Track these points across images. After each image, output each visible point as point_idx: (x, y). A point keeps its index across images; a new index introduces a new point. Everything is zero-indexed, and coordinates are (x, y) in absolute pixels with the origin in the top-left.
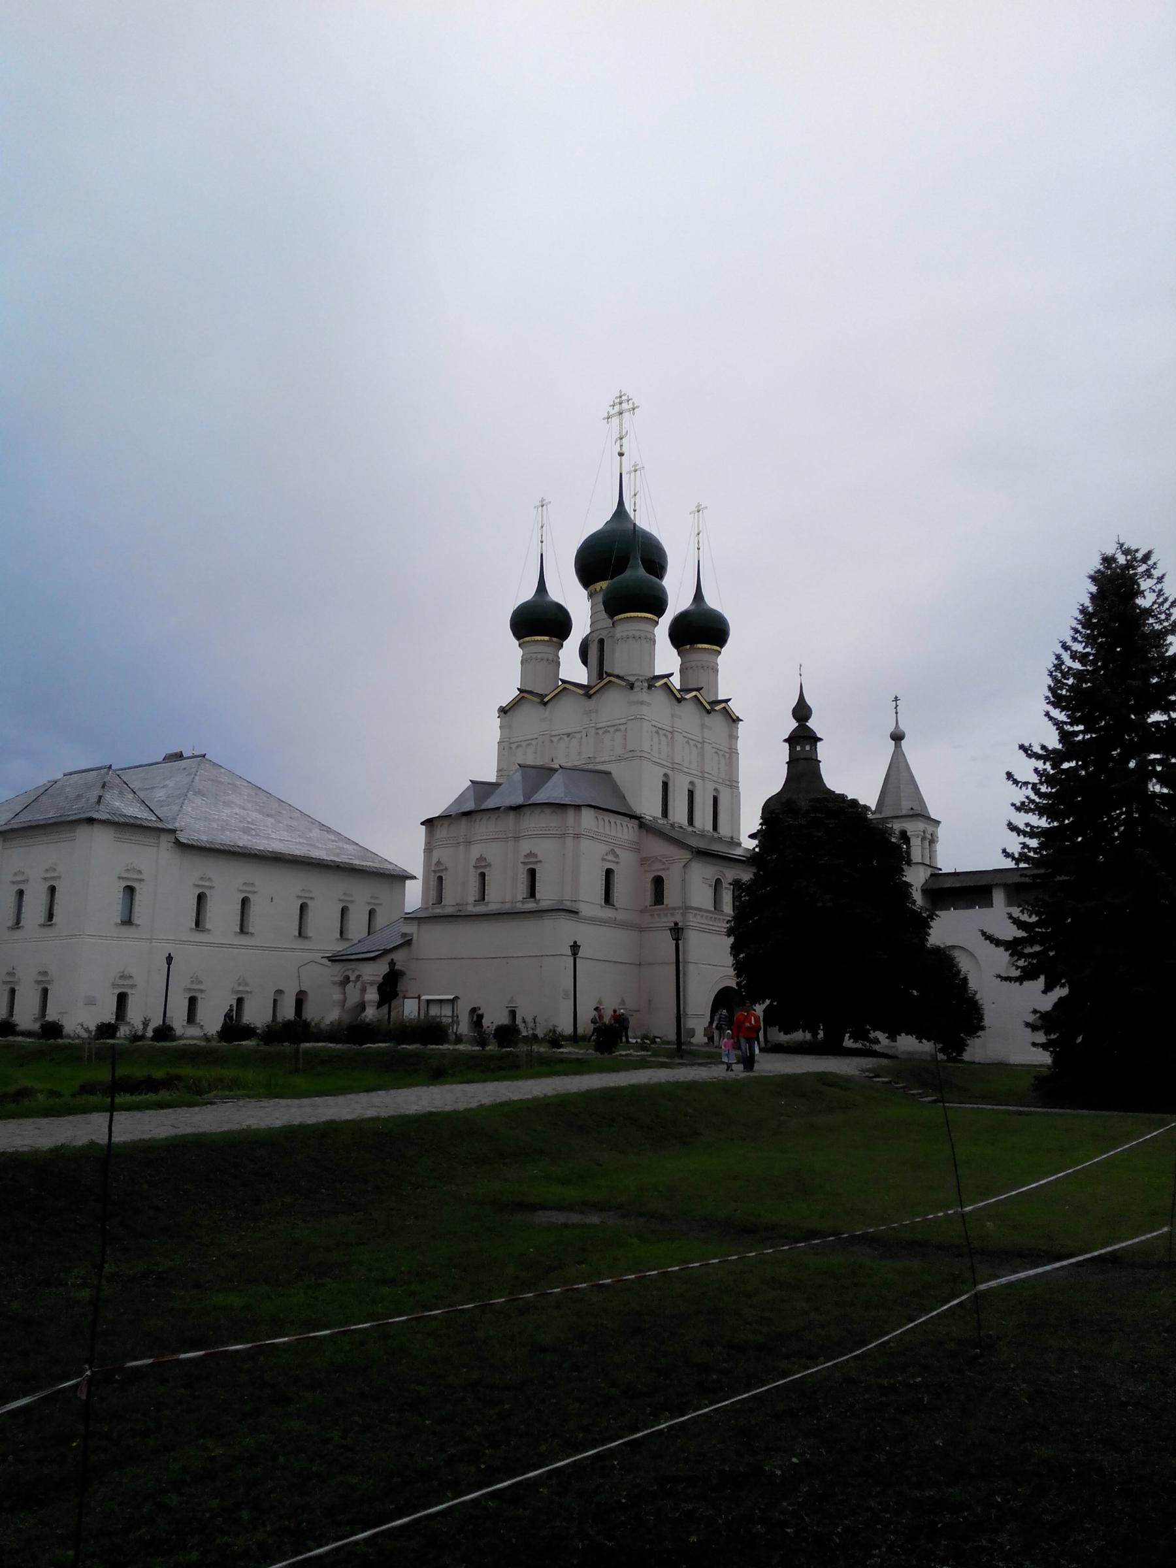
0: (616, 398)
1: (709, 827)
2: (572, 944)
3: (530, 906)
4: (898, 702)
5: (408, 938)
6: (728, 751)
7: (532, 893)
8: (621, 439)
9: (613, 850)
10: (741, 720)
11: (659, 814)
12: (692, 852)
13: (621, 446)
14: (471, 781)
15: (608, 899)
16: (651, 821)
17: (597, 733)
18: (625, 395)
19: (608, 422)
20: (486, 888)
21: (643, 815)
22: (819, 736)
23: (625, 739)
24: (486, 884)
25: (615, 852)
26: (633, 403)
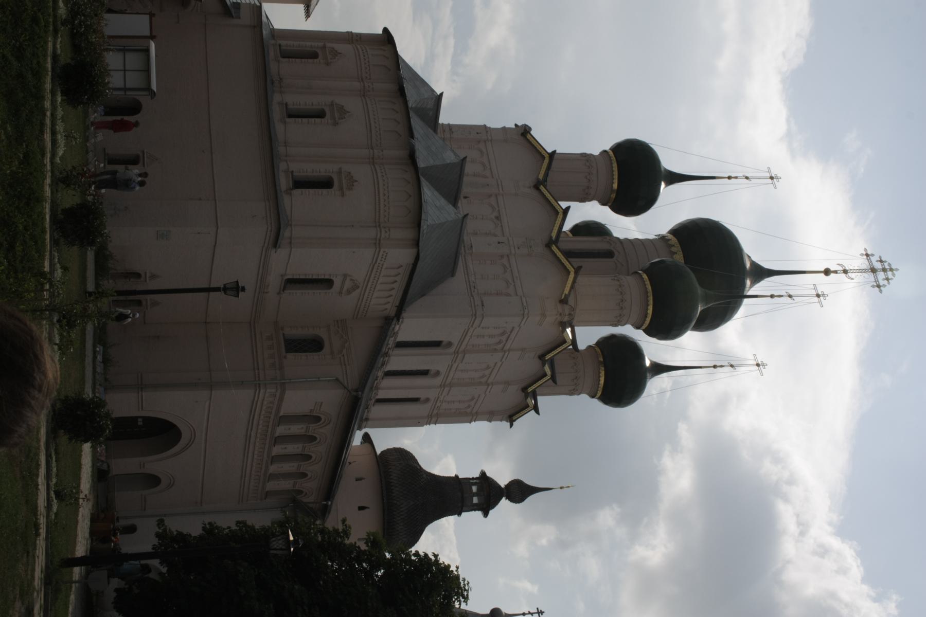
0: (889, 265)
1: (382, 395)
2: (241, 285)
3: (284, 182)
4: (537, 615)
5: (233, 11)
6: (475, 411)
7: (301, 184)
8: (845, 272)
9: (358, 287)
10: (511, 425)
11: (401, 337)
12: (357, 391)
13: (836, 272)
14: (442, 94)
15: (292, 283)
16: (393, 329)
17: (502, 257)
18: (894, 275)
19: (862, 255)
20: (305, 120)
21: (401, 320)
22: (491, 512)
23: (497, 294)
24: (310, 120)
25: (354, 290)
26: (884, 286)
